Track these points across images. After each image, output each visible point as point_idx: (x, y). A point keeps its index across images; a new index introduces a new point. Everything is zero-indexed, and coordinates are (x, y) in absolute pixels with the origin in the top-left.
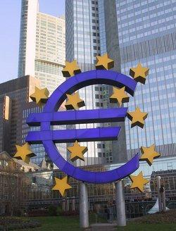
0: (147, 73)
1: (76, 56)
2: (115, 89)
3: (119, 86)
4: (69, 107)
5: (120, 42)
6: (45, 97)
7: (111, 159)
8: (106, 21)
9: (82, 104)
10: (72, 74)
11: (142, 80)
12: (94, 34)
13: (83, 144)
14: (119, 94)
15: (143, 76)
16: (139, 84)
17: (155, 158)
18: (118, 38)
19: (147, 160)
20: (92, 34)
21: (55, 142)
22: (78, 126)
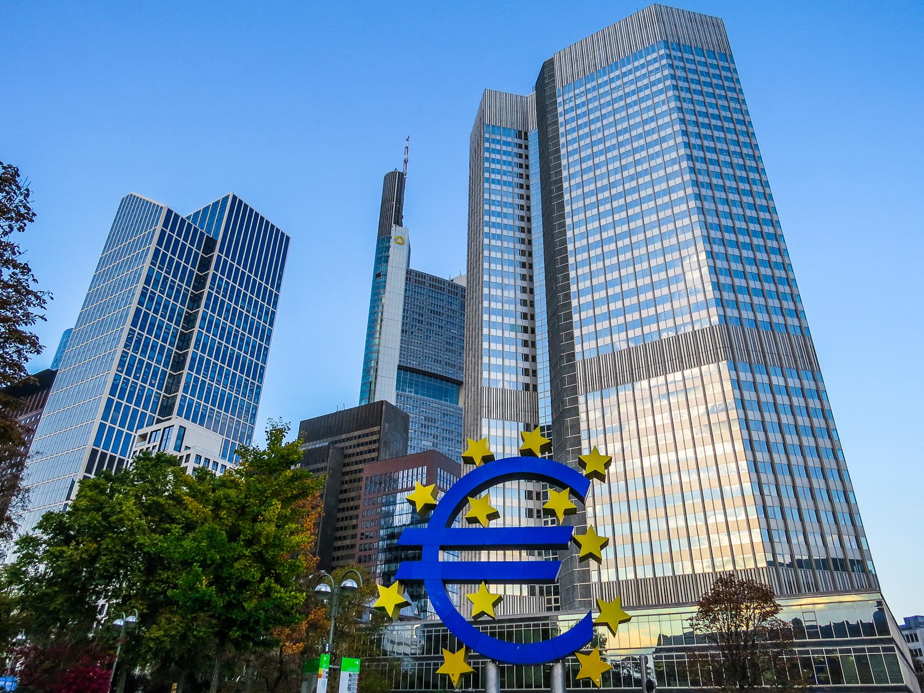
0: (607, 465)
1: (485, 374)
2: (551, 492)
3: (559, 485)
4: (474, 520)
5: (578, 348)
7: (556, 601)
8: (548, 304)
9: (494, 516)
10: (478, 461)
11: (602, 478)
12: (526, 372)
13: (496, 589)
14: (559, 500)
15: (601, 469)
16: (596, 481)
17: (620, 622)
18: (572, 338)
19: (606, 624)
20: (520, 343)
21: (445, 582)
22: (484, 556)
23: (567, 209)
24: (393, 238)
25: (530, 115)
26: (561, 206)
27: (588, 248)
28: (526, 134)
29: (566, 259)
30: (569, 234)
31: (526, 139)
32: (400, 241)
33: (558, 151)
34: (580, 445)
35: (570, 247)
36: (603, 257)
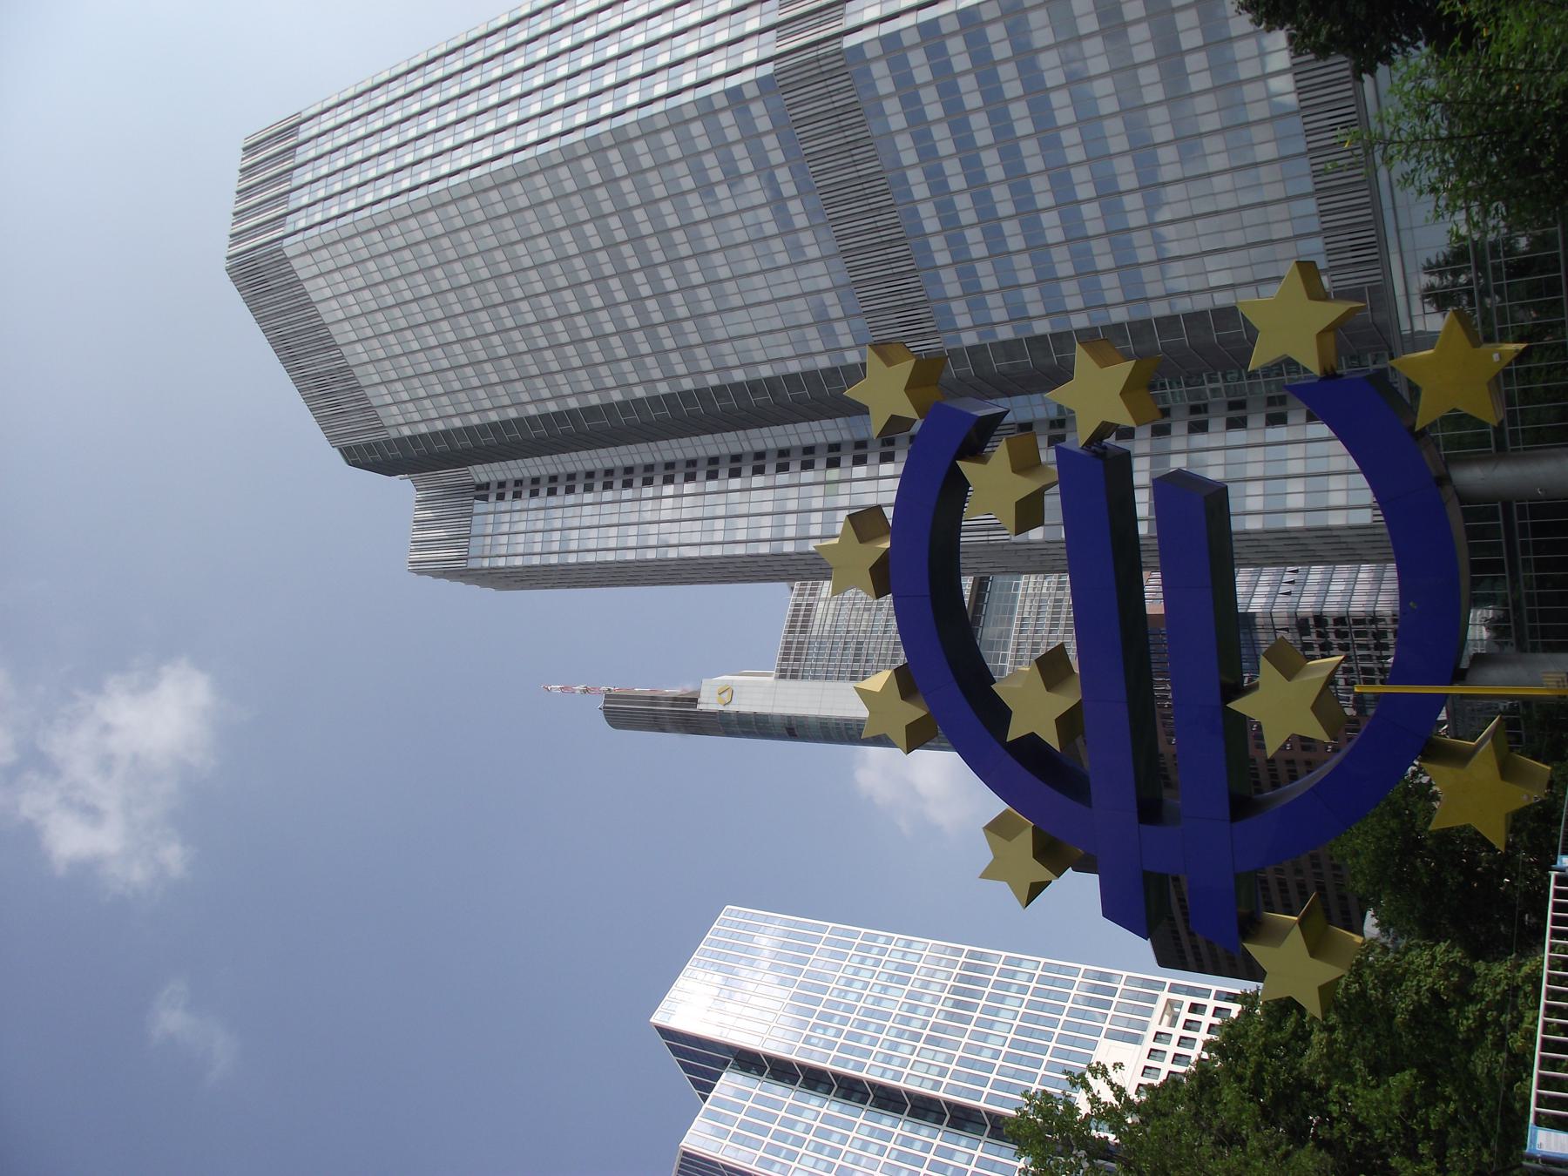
4: (1067, 723)
6: (1026, 839)
18: (834, 370)
23: (594, 400)
24: (721, 708)
25: (447, 482)
26: (590, 411)
27: (659, 353)
28: (480, 487)
29: (686, 395)
30: (639, 392)
31: (487, 486)
32: (726, 696)
33: (493, 426)
34: (1044, 337)
35: (663, 388)
36: (672, 322)
